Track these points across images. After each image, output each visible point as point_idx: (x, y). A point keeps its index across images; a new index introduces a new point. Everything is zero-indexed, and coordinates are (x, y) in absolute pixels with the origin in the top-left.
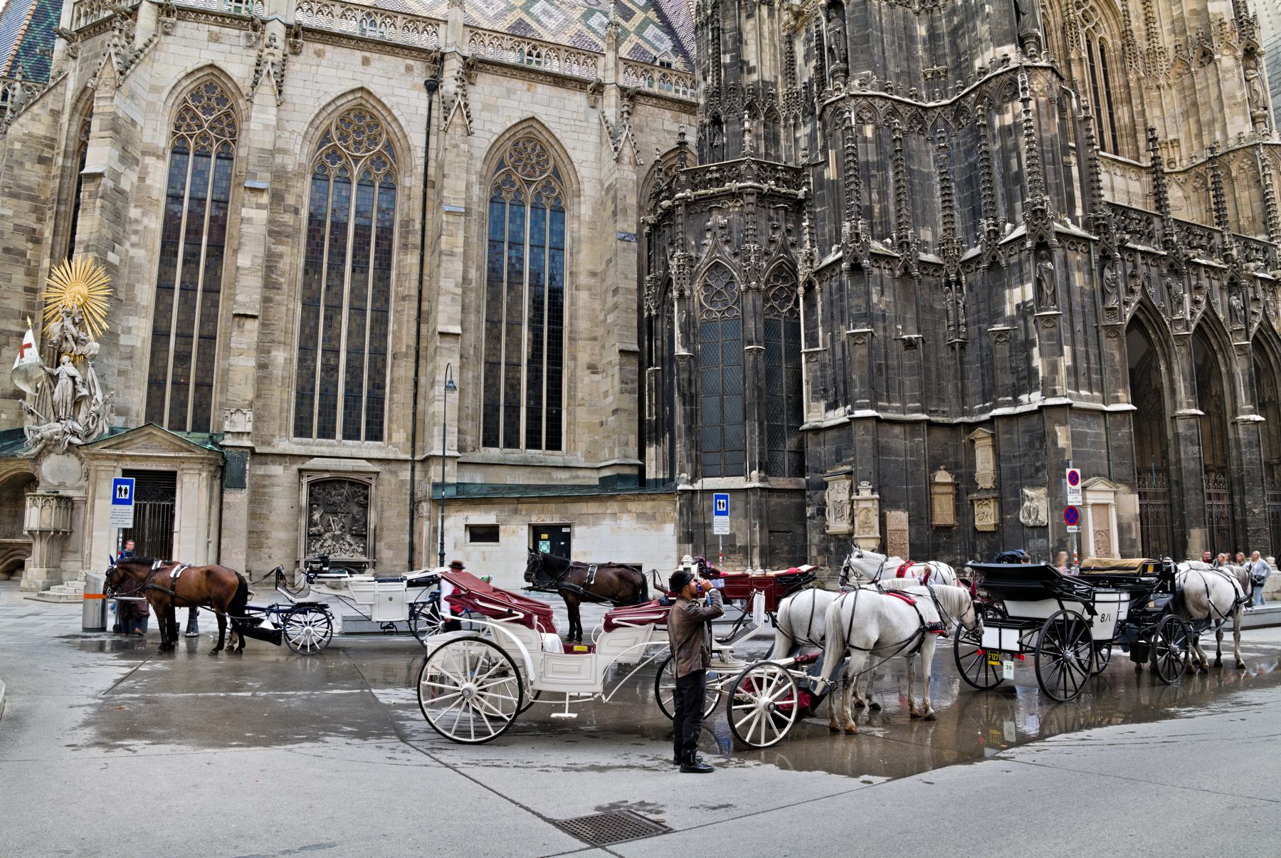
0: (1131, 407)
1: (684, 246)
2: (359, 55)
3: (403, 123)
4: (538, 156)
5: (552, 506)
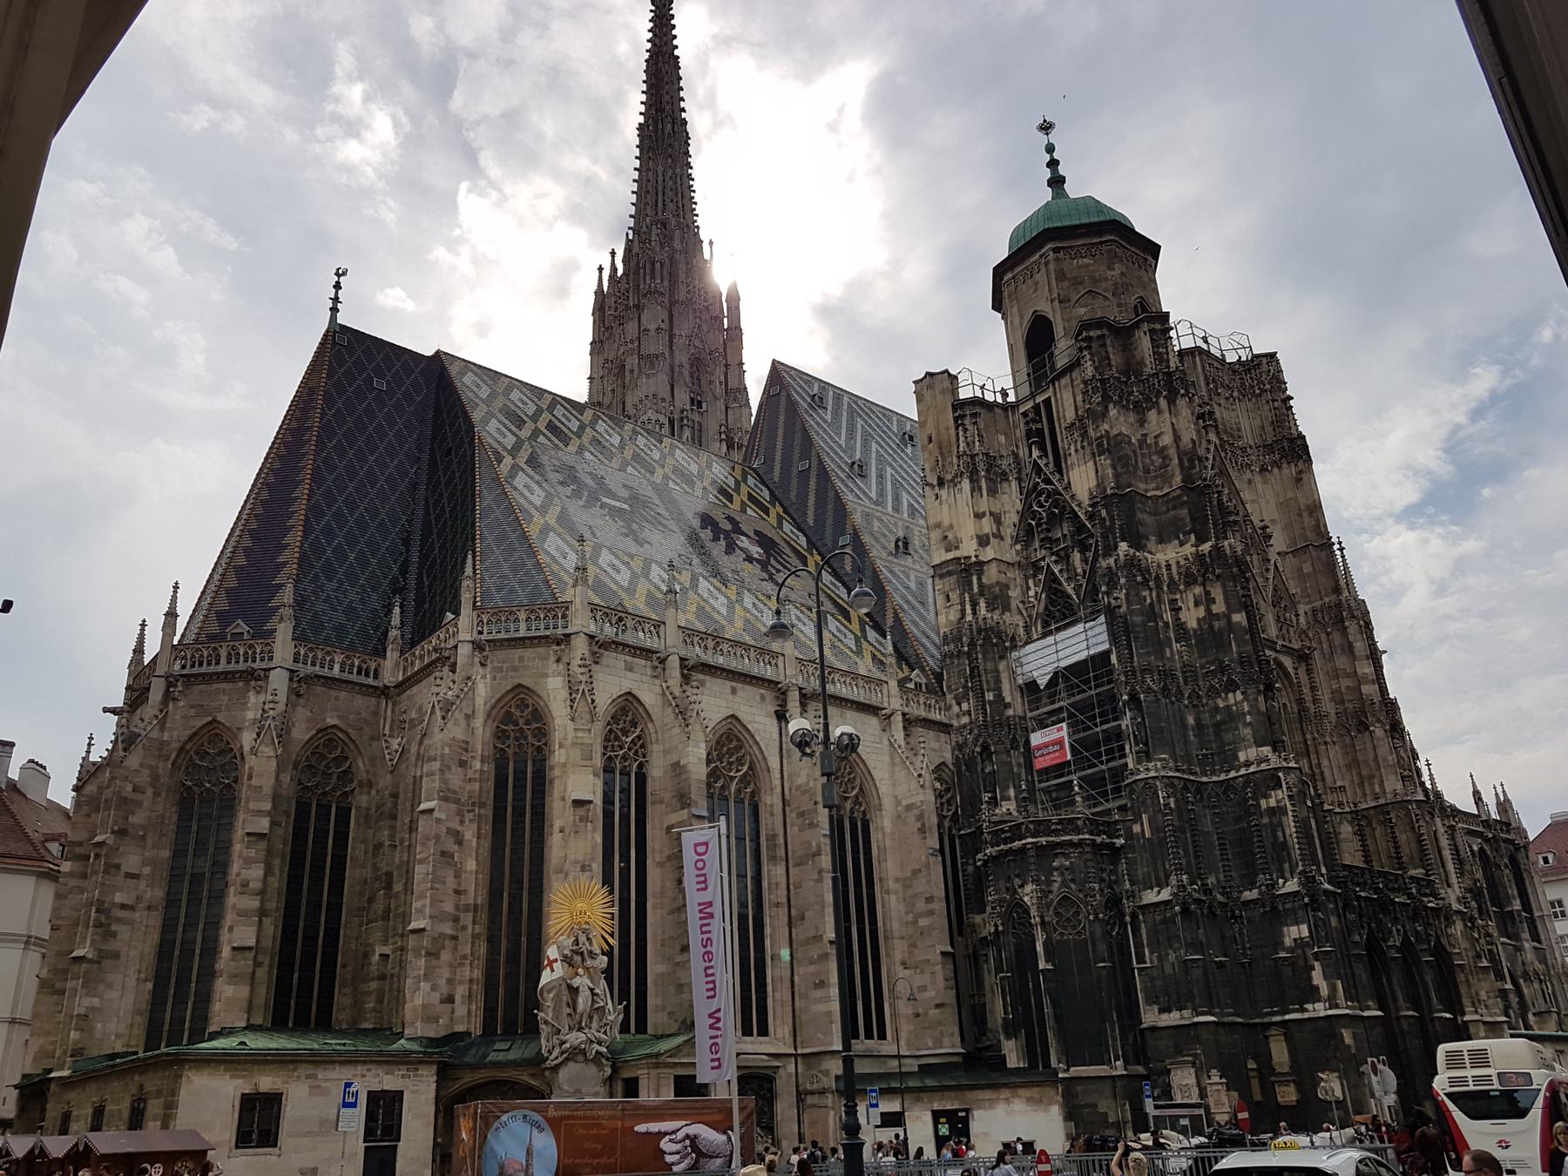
0: (1379, 1013)
1: (1037, 881)
2: (729, 684)
3: (763, 747)
5: (952, 1094)
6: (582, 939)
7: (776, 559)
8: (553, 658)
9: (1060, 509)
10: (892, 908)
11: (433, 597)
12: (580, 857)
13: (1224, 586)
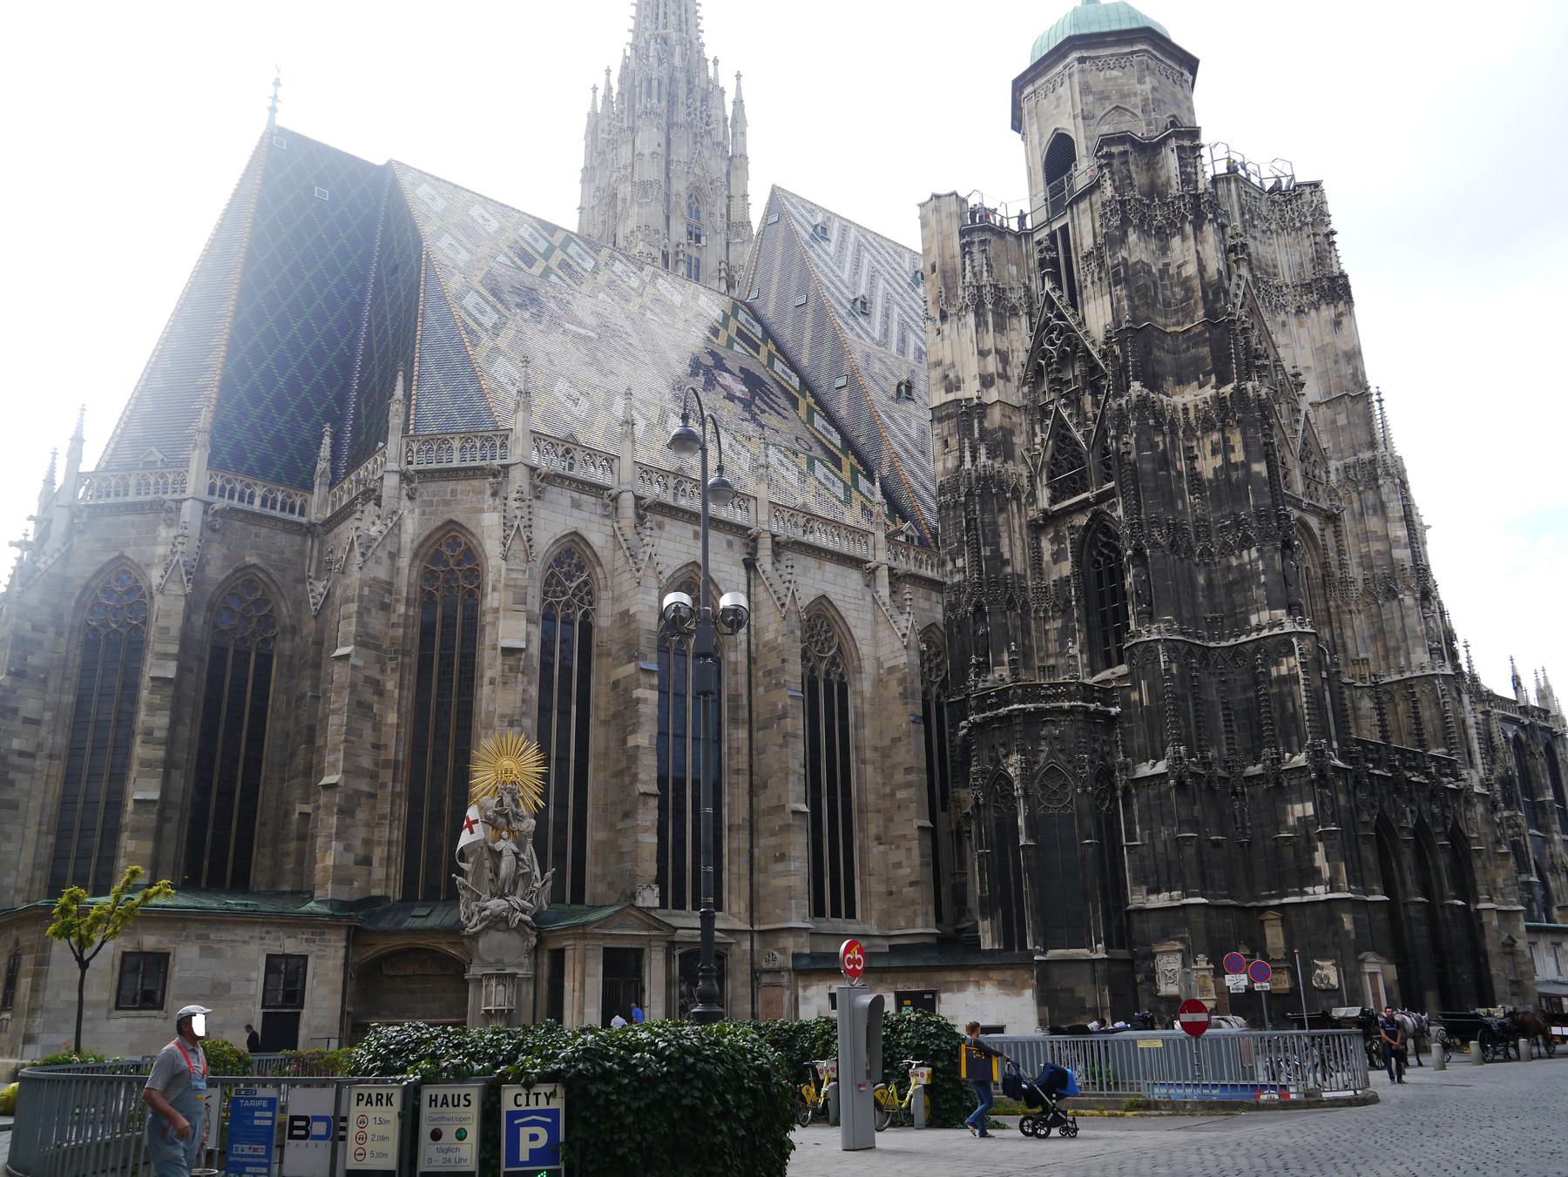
0: (1385, 898)
1: (1022, 751)
4: (826, 632)
6: (507, 799)
7: (761, 399)
8: (488, 492)
9: (1073, 348)
10: (867, 778)
11: (370, 428)
12: (508, 711)
13: (1244, 433)
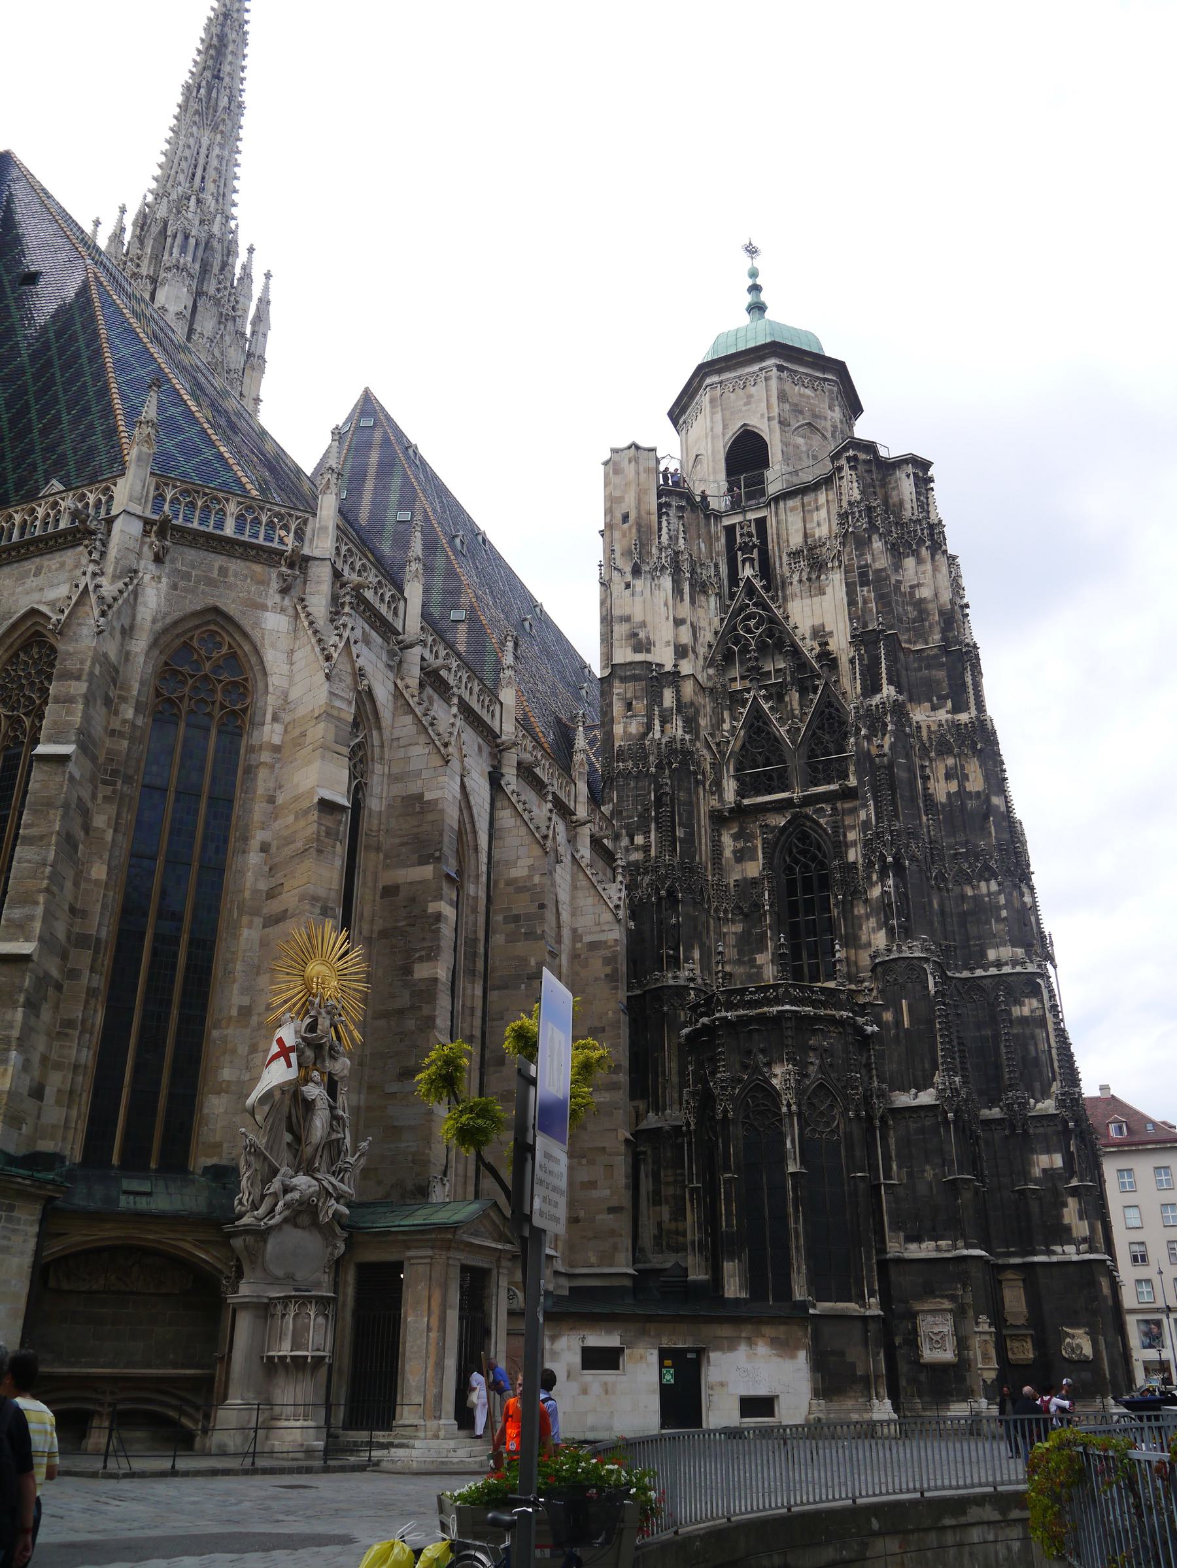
6: (324, 1023)
8: (275, 585)
